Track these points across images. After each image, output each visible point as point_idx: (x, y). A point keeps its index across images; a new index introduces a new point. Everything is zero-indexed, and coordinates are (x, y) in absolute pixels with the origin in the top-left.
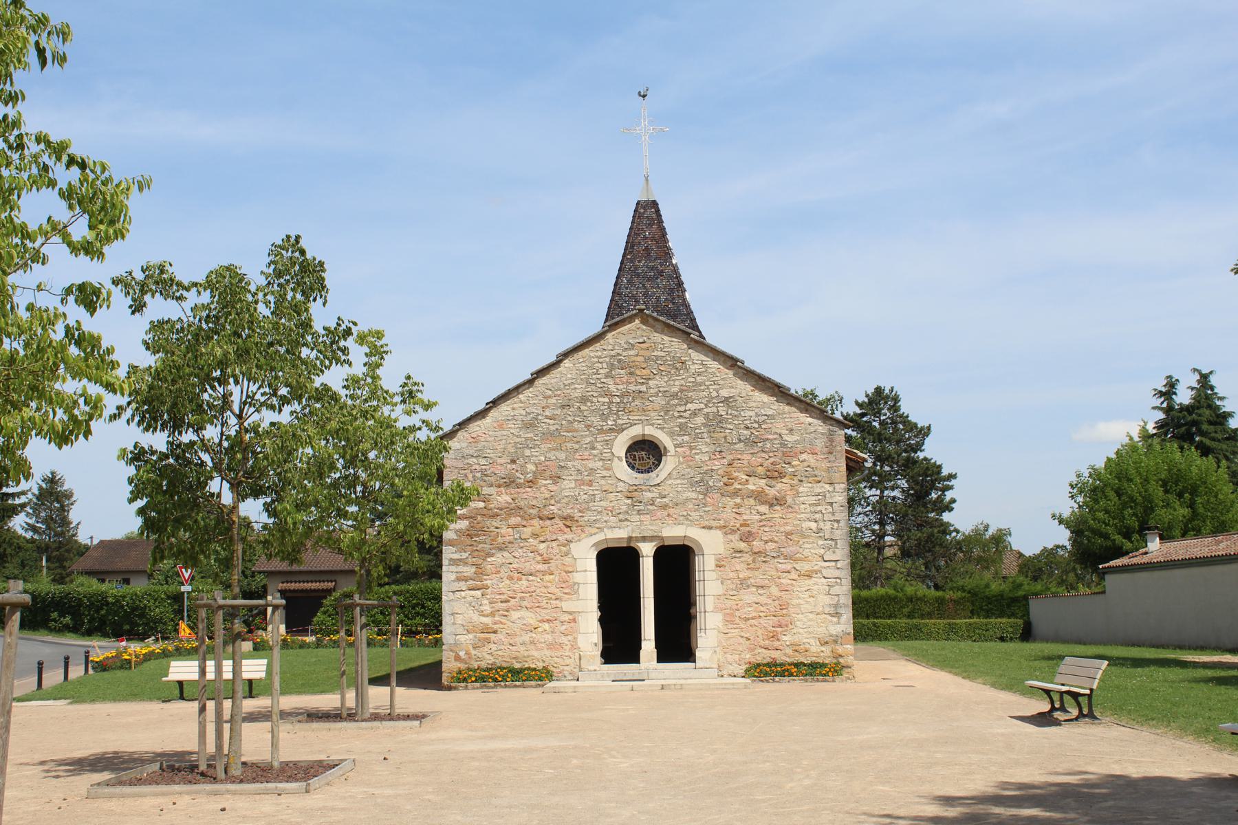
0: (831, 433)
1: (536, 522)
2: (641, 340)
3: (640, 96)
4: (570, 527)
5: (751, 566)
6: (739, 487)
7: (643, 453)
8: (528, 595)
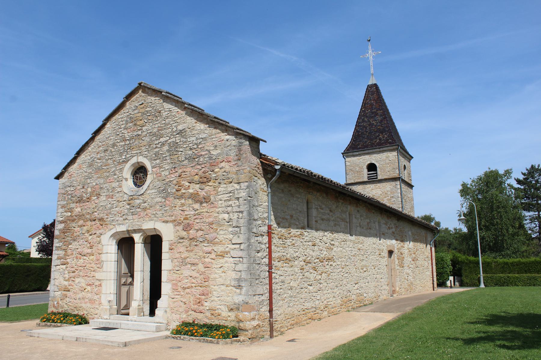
0: (240, 144)
1: (89, 223)
2: (141, 103)
3: (368, 41)
4: (102, 225)
5: (189, 249)
6: (183, 191)
7: (141, 174)
8: (83, 268)
